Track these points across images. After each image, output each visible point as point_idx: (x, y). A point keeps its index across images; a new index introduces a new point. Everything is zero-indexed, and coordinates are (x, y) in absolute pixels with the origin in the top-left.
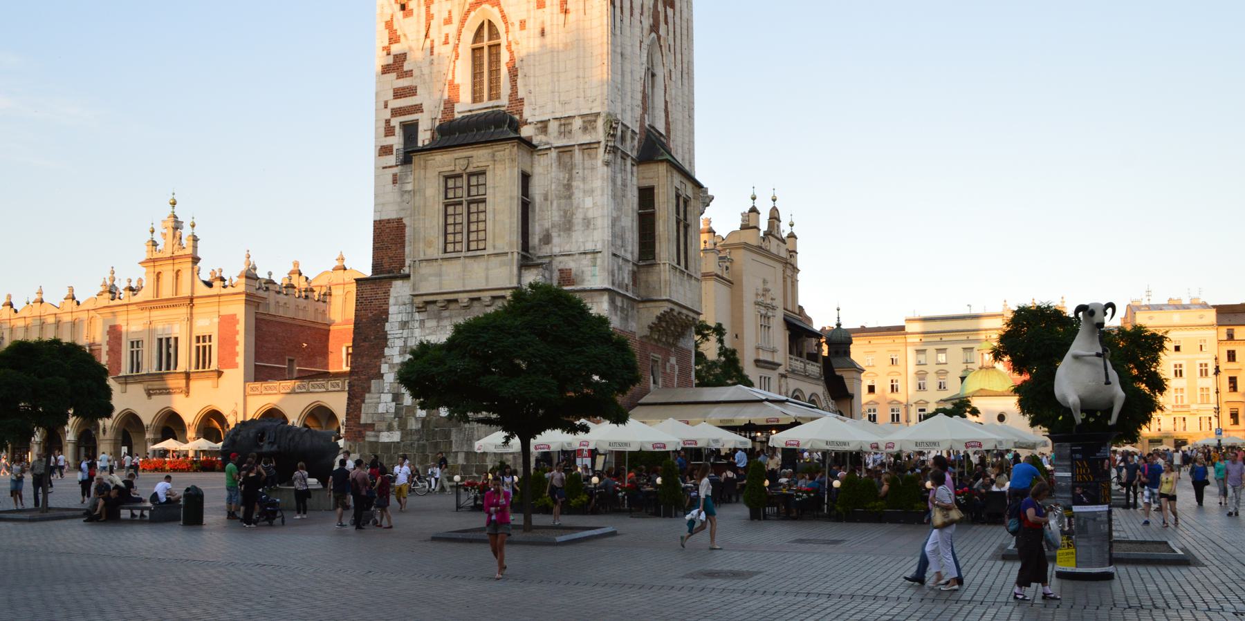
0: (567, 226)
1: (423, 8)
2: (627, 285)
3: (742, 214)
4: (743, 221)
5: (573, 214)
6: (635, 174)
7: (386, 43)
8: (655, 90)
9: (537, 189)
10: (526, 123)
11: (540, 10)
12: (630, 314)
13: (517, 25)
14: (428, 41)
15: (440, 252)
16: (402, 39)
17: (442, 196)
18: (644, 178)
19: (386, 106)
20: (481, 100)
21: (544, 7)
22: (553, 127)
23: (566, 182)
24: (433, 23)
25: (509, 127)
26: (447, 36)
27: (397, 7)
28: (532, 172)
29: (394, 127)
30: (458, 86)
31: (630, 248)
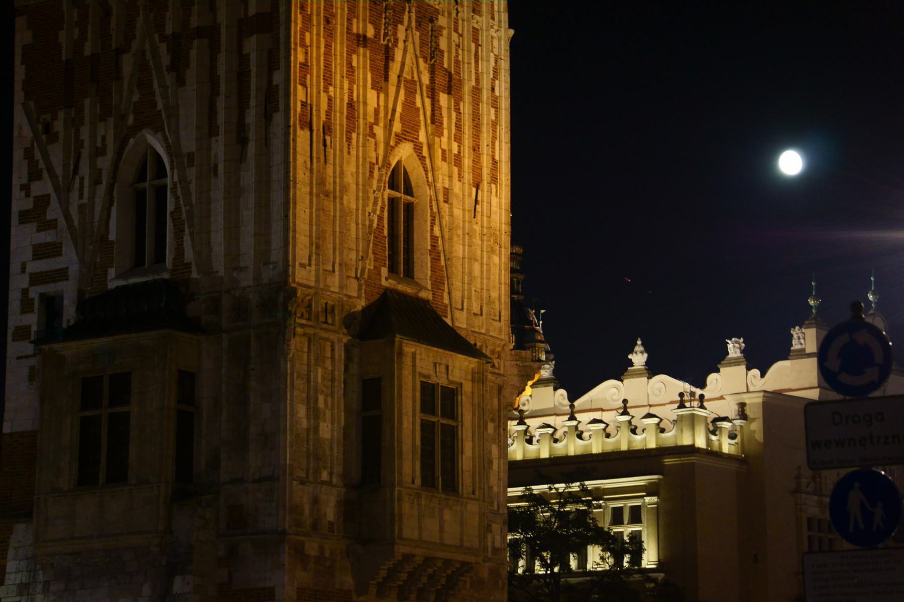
29: (33, 299)
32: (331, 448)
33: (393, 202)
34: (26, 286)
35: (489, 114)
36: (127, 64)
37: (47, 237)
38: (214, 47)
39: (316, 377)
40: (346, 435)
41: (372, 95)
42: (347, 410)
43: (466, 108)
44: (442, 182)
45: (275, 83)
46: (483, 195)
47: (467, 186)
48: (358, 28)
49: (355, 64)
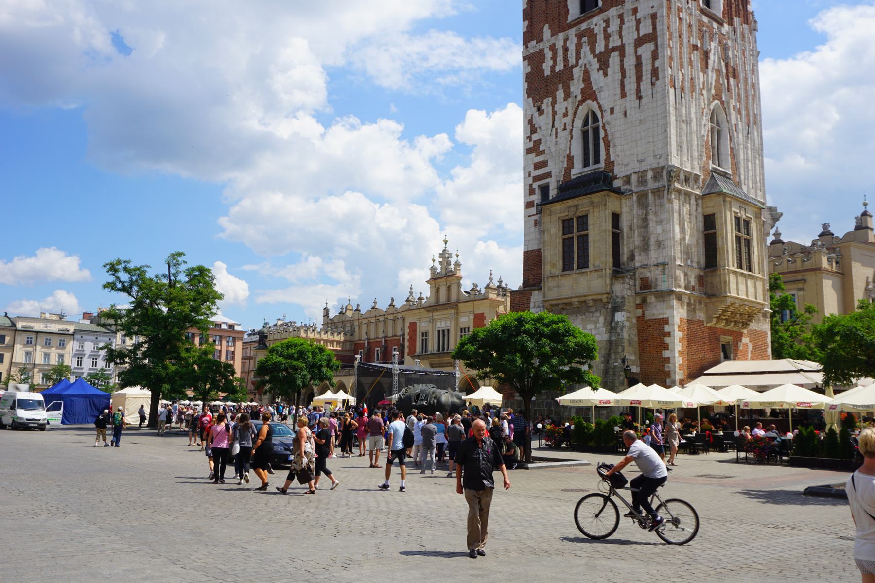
0: (645, 247)
1: (550, 108)
2: (693, 287)
3: (856, 218)
4: (857, 223)
5: (649, 238)
6: (700, 205)
7: (529, 134)
8: (722, 141)
9: (624, 224)
10: (616, 178)
11: (623, 99)
12: (697, 307)
13: (609, 111)
15: (560, 271)
16: (538, 130)
18: (707, 207)
20: (589, 165)
21: (626, 97)
22: (634, 178)
23: (643, 216)
24: (556, 117)
25: (603, 182)
26: (565, 124)
27: (536, 109)
28: (621, 211)
30: (573, 157)
31: (695, 260)
32: (691, 248)
33: (712, 128)
34: (531, 182)
35: (751, 91)
36: (577, 72)
37: (540, 158)
38: (622, 55)
39: (683, 212)
40: (697, 243)
41: (701, 75)
42: (698, 230)
43: (741, 86)
44: (733, 122)
45: (656, 66)
46: (751, 130)
47: (744, 124)
48: (693, 41)
49: (692, 59)
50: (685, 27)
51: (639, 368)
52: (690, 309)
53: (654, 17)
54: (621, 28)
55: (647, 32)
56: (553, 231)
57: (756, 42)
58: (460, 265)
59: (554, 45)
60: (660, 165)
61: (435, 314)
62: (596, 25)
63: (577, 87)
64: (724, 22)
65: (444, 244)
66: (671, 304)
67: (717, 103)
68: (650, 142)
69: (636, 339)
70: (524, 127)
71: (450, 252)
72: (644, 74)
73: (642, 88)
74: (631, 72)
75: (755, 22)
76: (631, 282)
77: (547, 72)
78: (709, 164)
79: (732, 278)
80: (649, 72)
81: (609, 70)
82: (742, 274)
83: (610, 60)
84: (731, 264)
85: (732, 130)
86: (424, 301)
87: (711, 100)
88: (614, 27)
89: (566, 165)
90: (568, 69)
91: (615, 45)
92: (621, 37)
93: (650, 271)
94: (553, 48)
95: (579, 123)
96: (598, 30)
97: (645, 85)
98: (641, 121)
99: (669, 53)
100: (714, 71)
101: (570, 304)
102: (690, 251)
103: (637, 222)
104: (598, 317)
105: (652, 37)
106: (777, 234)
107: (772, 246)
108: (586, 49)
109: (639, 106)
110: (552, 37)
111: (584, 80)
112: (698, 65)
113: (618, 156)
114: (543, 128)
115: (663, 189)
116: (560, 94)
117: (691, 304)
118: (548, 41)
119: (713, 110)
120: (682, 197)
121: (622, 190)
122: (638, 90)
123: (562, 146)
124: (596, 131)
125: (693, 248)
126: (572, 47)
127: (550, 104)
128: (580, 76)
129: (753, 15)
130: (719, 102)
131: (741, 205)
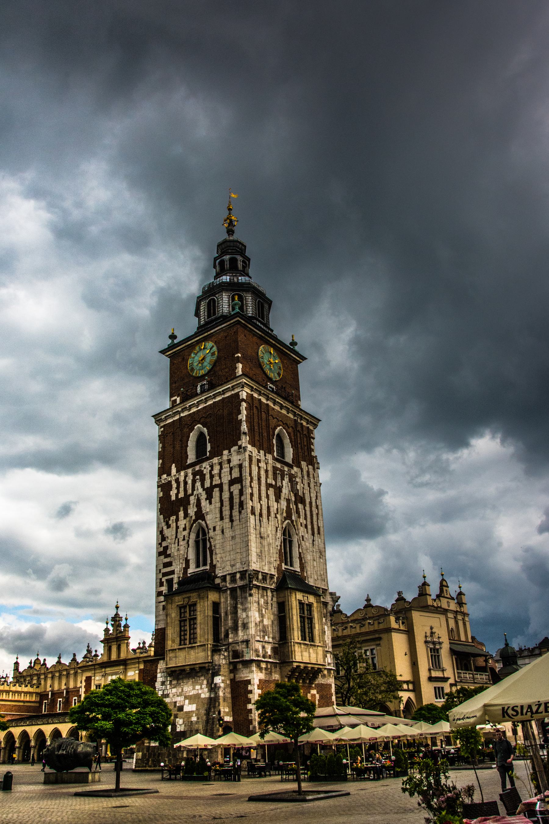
0: (235, 629)
1: (175, 524)
2: (270, 655)
3: (419, 587)
4: (419, 591)
7: (160, 542)
12: (273, 671)
13: (212, 528)
14: (177, 539)
17: (179, 617)
18: (280, 597)
19: (160, 572)
20: (200, 567)
21: (223, 520)
22: (228, 578)
23: (234, 605)
26: (184, 536)
28: (220, 601)
29: (163, 582)
30: (189, 560)
31: (271, 636)
32: (268, 628)
34: (161, 577)
35: (315, 511)
36: (192, 499)
37: (167, 560)
38: (221, 491)
41: (275, 504)
43: (308, 508)
49: (269, 493)
50: (263, 473)
51: (232, 718)
52: (267, 672)
53: (240, 466)
54: (220, 471)
55: (236, 477)
56: (173, 615)
57: (318, 477)
58: (128, 627)
59: (178, 478)
60: (244, 569)
61: (107, 669)
62: (205, 468)
63: (192, 511)
64: (293, 466)
65: (116, 609)
66: (252, 669)
67: (288, 523)
68: (238, 553)
69: (229, 695)
70: (157, 536)
71: (120, 616)
72: (234, 505)
73: (233, 514)
74: (226, 503)
75: (318, 463)
76: (226, 654)
77: (173, 498)
78: (282, 566)
79: (297, 648)
80: (238, 504)
81: (213, 499)
82: (305, 644)
83: (214, 493)
84: (296, 638)
85: (300, 540)
86: (99, 658)
87: (283, 520)
88: (216, 471)
89: (184, 566)
90: (187, 497)
91: (217, 483)
92: (220, 478)
93: (239, 646)
94: (177, 481)
95: (193, 536)
96: (206, 471)
97: (235, 513)
98: (233, 537)
99: (250, 491)
100: (285, 500)
101: (184, 670)
102: (267, 630)
103: (230, 609)
104: (203, 680)
105: (239, 480)
106: (368, 600)
107: (365, 609)
108: (198, 484)
109: (232, 527)
110: (177, 473)
111: (196, 506)
112: (272, 497)
113: (218, 561)
114: (170, 538)
115: (246, 586)
116: (181, 514)
117: (268, 669)
118: (175, 476)
119: (286, 527)
120: (261, 592)
121: (221, 586)
122: (231, 516)
123: (182, 552)
124: (204, 541)
125: (269, 628)
126: (190, 482)
127: (174, 520)
128: (194, 503)
129: (316, 458)
130: (290, 521)
131: (304, 595)
